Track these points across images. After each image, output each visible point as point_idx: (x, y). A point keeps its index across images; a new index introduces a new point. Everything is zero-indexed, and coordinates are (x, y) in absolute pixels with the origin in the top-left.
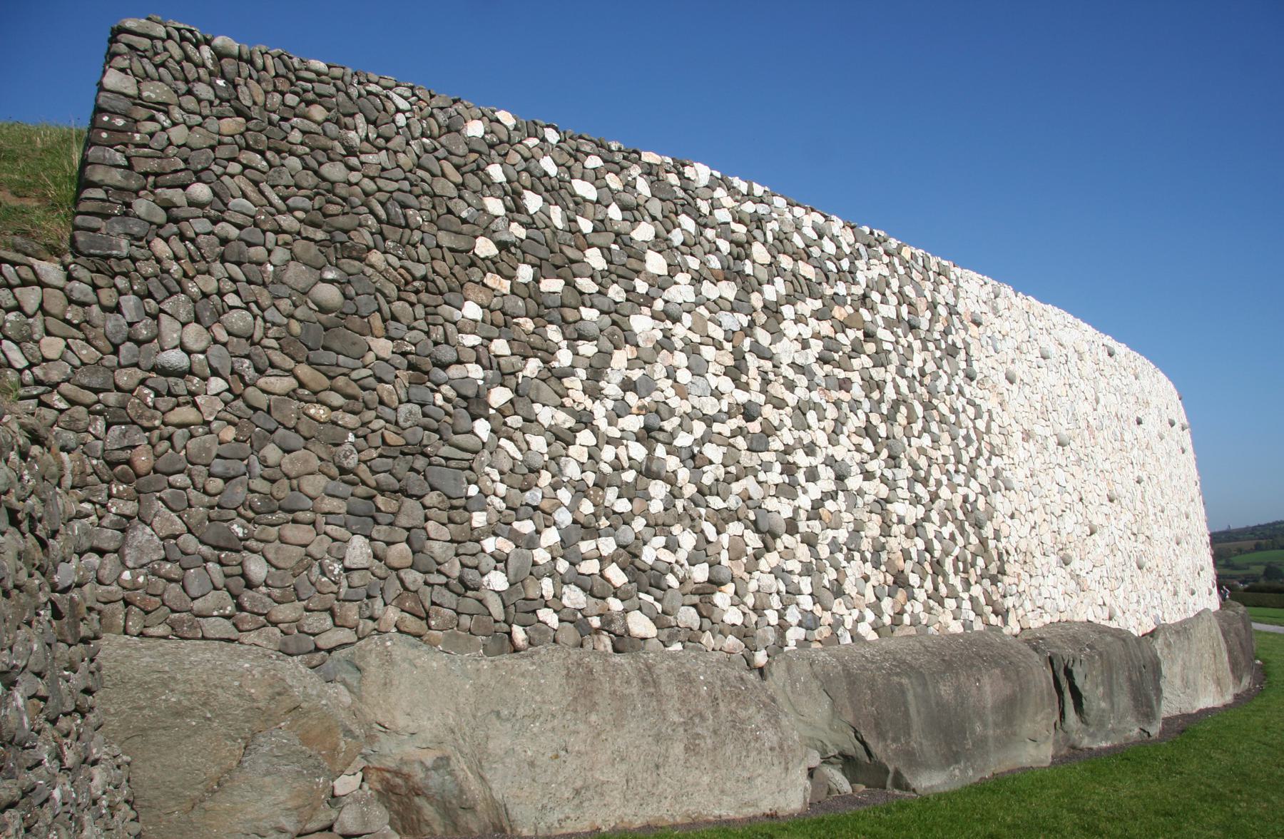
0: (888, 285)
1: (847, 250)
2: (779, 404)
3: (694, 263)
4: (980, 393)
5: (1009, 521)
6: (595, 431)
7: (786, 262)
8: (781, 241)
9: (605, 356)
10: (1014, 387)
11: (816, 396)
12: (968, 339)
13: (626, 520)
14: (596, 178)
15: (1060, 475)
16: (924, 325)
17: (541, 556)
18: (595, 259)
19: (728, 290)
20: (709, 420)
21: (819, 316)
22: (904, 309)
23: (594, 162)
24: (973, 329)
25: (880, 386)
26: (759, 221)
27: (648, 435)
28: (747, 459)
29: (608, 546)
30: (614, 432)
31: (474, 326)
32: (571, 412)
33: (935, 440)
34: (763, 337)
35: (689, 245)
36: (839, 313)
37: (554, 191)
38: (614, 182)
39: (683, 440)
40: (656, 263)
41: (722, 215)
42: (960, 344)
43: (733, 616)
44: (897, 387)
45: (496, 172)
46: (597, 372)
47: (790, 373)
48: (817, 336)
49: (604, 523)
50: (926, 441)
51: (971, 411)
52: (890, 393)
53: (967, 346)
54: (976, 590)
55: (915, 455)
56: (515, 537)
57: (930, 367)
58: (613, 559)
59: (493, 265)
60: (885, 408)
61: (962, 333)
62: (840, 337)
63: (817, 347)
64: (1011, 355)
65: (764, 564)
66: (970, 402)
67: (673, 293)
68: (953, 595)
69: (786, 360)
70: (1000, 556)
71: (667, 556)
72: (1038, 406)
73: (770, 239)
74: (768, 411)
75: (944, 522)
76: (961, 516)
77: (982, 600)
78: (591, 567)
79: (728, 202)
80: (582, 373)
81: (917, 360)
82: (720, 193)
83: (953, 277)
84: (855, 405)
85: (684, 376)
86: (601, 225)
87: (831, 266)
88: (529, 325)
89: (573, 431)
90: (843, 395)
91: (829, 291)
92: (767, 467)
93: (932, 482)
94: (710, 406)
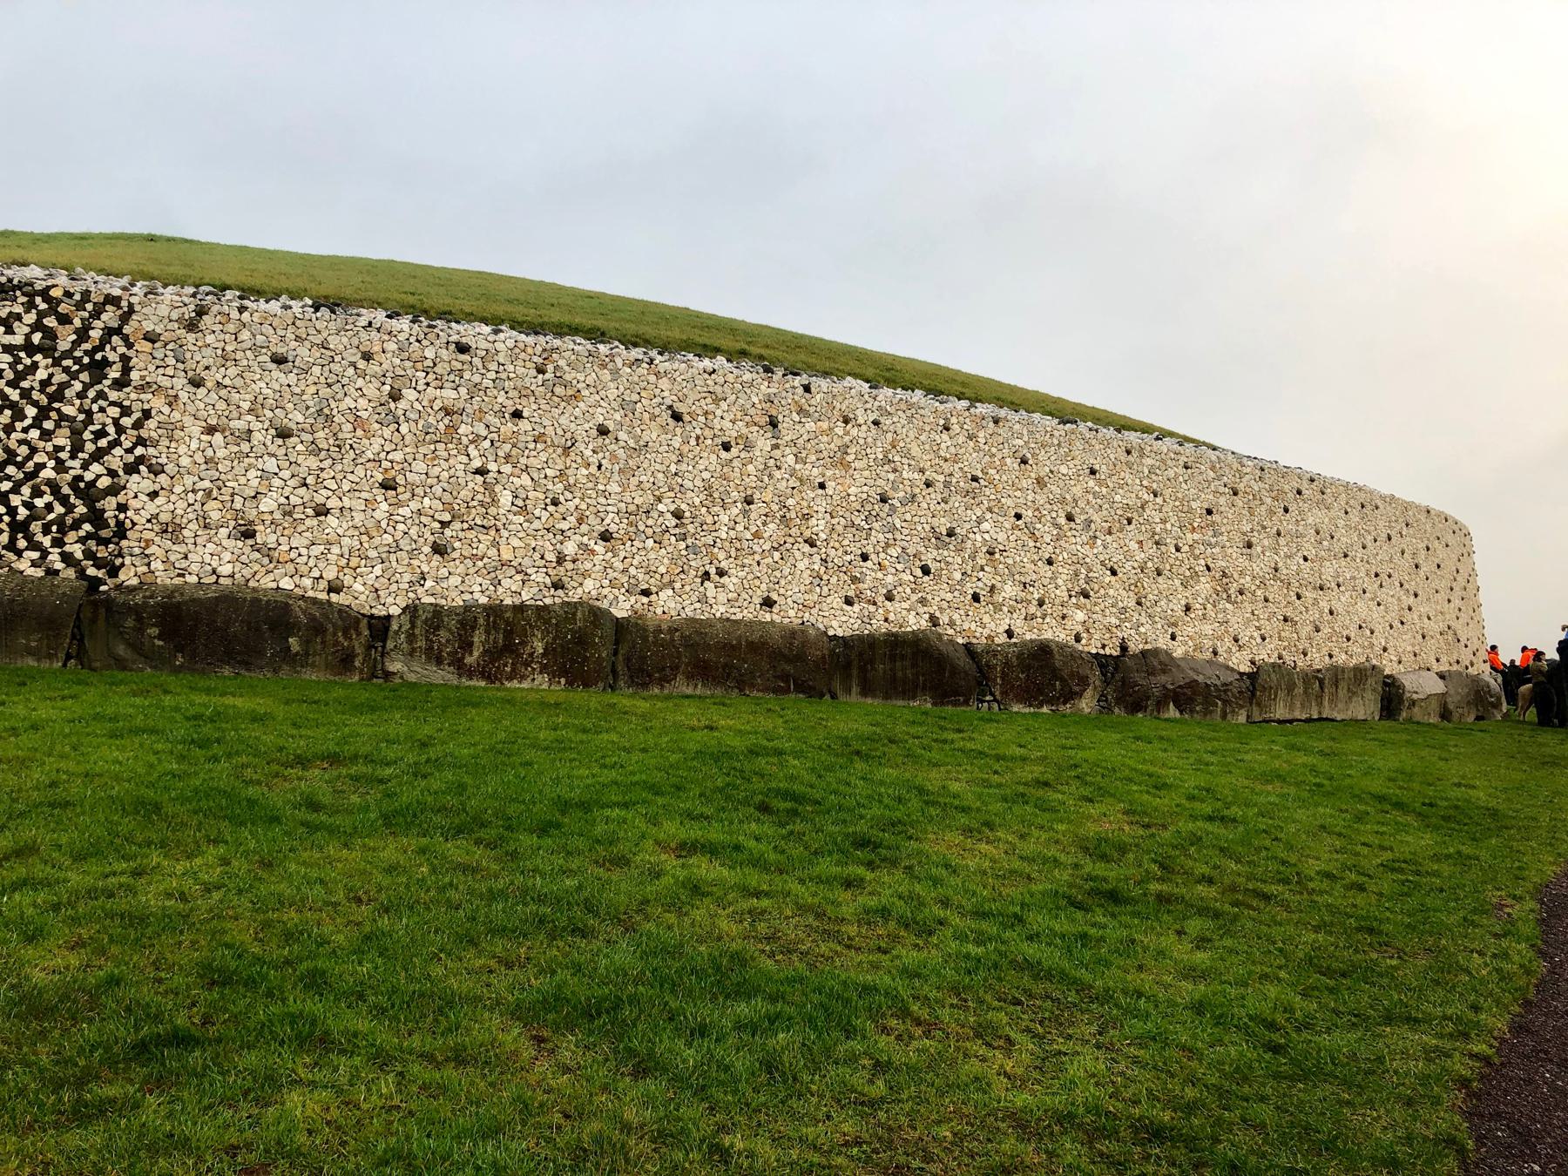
4: (133, 396)
5: (146, 499)
10: (202, 391)
12: (131, 353)
15: (271, 465)
16: (63, 345)
22: (37, 338)
24: (147, 346)
33: (46, 435)
42: (112, 357)
50: (34, 434)
51: (114, 412)
53: (125, 359)
54: (77, 551)
55: (13, 444)
57: (60, 377)
64: (205, 362)
66: (113, 404)
68: (34, 545)
70: (120, 524)
75: (37, 493)
76: (66, 490)
77: (79, 555)
81: (42, 374)
83: (124, 304)
93: (31, 464)
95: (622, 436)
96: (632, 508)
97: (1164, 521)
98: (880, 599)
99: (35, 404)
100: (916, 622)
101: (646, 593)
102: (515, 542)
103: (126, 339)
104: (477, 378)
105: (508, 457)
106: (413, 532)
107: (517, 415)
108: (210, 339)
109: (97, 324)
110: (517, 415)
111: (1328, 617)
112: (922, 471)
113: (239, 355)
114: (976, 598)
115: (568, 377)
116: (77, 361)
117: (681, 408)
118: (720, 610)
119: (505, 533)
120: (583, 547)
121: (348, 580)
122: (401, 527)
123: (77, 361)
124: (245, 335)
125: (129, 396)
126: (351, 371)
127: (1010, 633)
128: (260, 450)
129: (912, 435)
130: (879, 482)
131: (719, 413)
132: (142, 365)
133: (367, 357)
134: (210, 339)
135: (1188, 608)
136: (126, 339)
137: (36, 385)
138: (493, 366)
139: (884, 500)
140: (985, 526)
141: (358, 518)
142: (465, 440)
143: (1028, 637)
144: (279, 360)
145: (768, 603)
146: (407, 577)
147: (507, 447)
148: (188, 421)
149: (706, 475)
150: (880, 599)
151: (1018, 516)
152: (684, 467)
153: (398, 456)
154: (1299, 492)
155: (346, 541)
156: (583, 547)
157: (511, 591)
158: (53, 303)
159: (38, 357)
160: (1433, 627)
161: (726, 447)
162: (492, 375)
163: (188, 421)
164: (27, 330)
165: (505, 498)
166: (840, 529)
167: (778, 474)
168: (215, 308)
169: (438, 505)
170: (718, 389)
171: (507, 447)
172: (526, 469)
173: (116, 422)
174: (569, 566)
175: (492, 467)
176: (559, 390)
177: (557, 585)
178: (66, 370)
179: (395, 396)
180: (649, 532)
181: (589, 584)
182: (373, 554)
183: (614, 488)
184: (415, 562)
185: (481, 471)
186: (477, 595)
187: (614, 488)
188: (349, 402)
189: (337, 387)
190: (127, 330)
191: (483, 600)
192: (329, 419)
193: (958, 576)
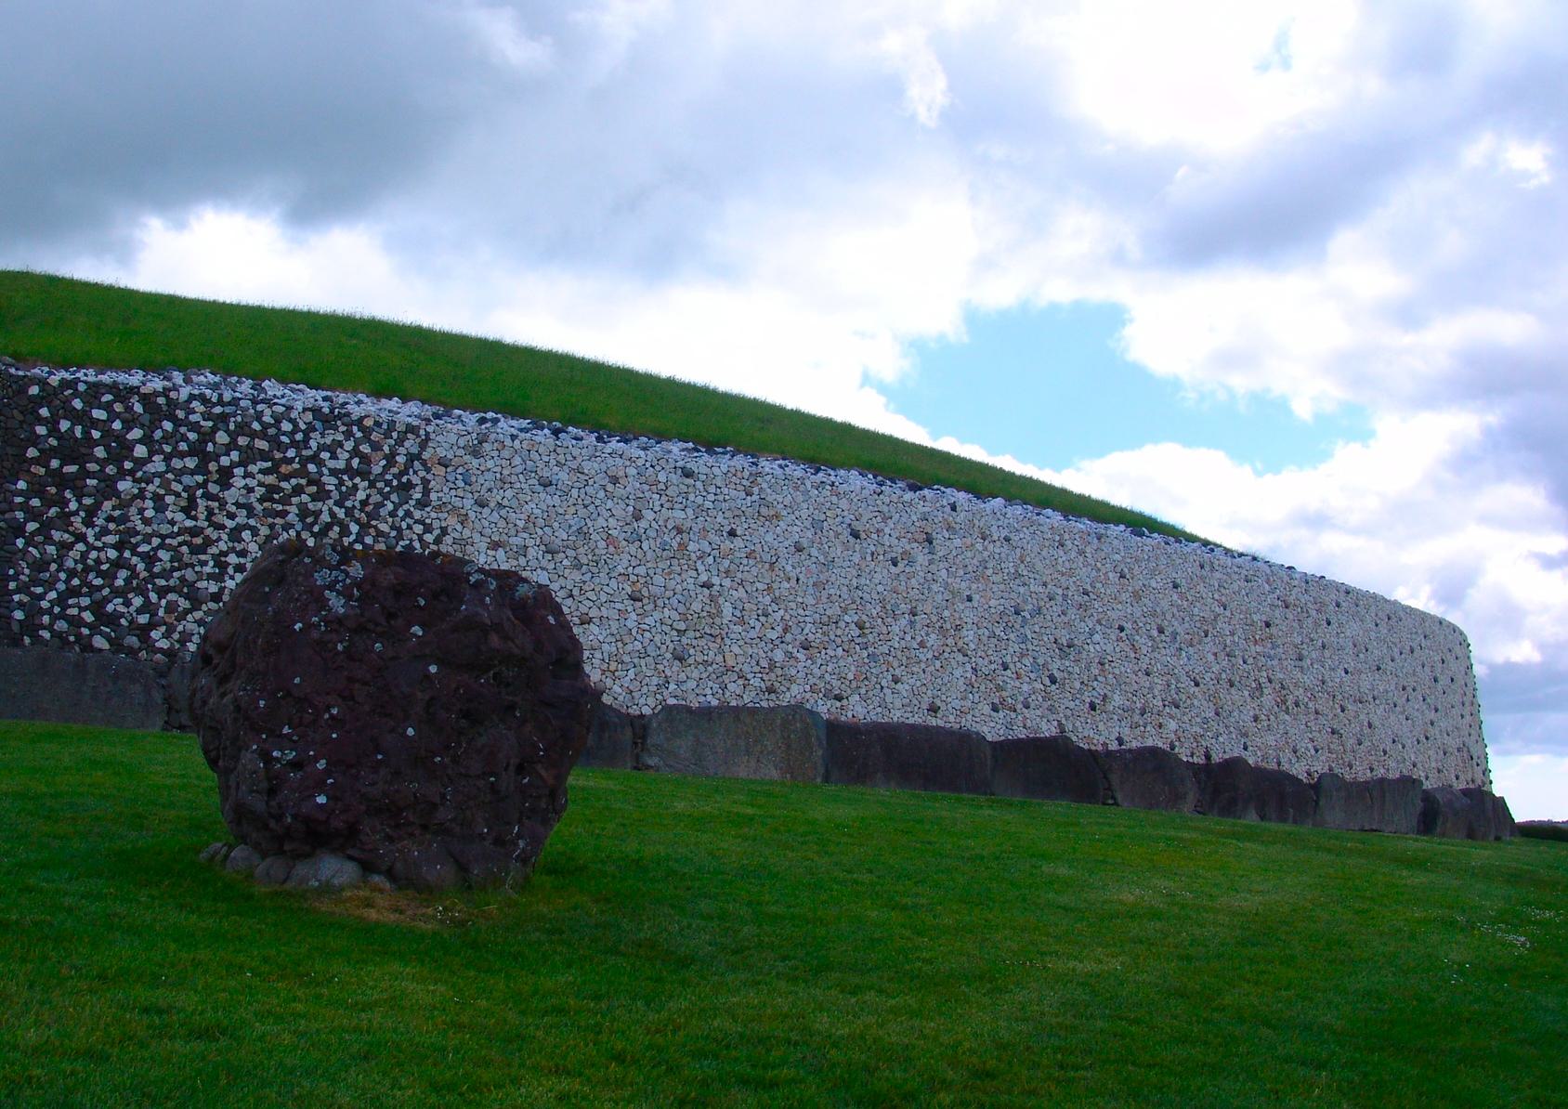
0: (341, 446)
1: (303, 427)
2: (223, 527)
3: (168, 449)
4: (433, 515)
6: (87, 543)
7: (242, 441)
8: (243, 429)
9: (98, 506)
10: (486, 511)
11: (252, 522)
12: (429, 477)
13: (100, 588)
14: (108, 407)
16: (377, 469)
17: (45, 604)
18: (100, 452)
19: (191, 463)
20: (163, 537)
21: (264, 472)
22: (355, 462)
23: (107, 398)
24: (440, 470)
25: (317, 514)
26: (224, 418)
27: (119, 547)
28: (186, 559)
29: (85, 601)
30: (99, 544)
31: (20, 493)
32: (71, 534)
34: (213, 488)
35: (167, 438)
36: (284, 469)
37: (81, 417)
38: (118, 407)
39: (144, 548)
40: (140, 451)
41: (193, 418)
42: (416, 480)
43: (164, 644)
44: (332, 514)
45: (44, 412)
46: (92, 512)
47: (233, 509)
48: (261, 484)
49: (85, 590)
51: (418, 529)
52: (325, 518)
53: (425, 482)
56: (32, 595)
57: (376, 498)
58: (86, 609)
59: (35, 461)
60: (316, 529)
61: (422, 474)
62: (284, 485)
63: (260, 491)
64: (487, 485)
65: (189, 617)
66: (417, 522)
67: (150, 468)
69: (230, 501)
71: (122, 609)
72: (521, 524)
73: (232, 427)
74: (209, 531)
78: (74, 611)
79: (202, 408)
80: (82, 514)
81: (361, 495)
82: (195, 404)
84: (287, 527)
85: (149, 513)
86: (108, 433)
87: (285, 439)
88: (53, 490)
89: (73, 544)
90: (279, 521)
91: (278, 455)
92: (204, 563)
94: (165, 529)
95: (814, 552)
96: (825, 619)
97: (1232, 634)
98: (1019, 706)
99: (358, 522)
100: (1048, 730)
101: (839, 698)
102: (736, 649)
103: (424, 463)
104: (699, 499)
105: (727, 572)
106: (657, 639)
107: (732, 533)
108: (490, 464)
109: (402, 450)
110: (732, 533)
111: (1367, 730)
112: (1045, 584)
113: (514, 478)
114: (1092, 706)
115: (769, 499)
116: (388, 483)
117: (857, 526)
118: (896, 716)
119: (728, 642)
120: (790, 655)
121: (609, 682)
122: (647, 635)
123: (388, 483)
124: (517, 461)
125: (430, 515)
126: (602, 494)
127: (1120, 741)
128: (533, 563)
129: (1036, 549)
130: (1014, 595)
131: (887, 530)
132: (438, 487)
133: (615, 480)
134: (490, 464)
135: (1256, 719)
136: (424, 463)
137: (357, 504)
138: (712, 489)
139: (1017, 613)
140: (1097, 637)
141: (614, 625)
142: (693, 557)
143: (1134, 744)
144: (546, 484)
145: (933, 709)
146: (655, 681)
147: (726, 563)
148: (477, 537)
149: (880, 588)
150: (1019, 706)
151: (1121, 629)
152: (863, 581)
153: (641, 570)
154: (1338, 605)
155: (605, 647)
156: (790, 655)
157: (737, 694)
158: (367, 432)
159: (357, 480)
160: (1452, 743)
161: (895, 564)
162: (711, 497)
163: (477, 537)
164: (347, 455)
165: (727, 610)
166: (984, 639)
167: (935, 587)
168: (493, 436)
169: (675, 616)
170: (885, 509)
171: (726, 563)
172: (741, 584)
173: (421, 539)
174: (779, 672)
175: (716, 580)
176: (764, 511)
177: (771, 690)
178: (380, 492)
179: (638, 517)
180: (838, 641)
181: (795, 689)
182: (627, 659)
183: (810, 600)
184: (661, 667)
185: (707, 585)
186: (709, 698)
187: (810, 600)
188: (601, 522)
189: (591, 508)
190: (425, 455)
191: (715, 703)
192: (587, 536)
193: (1077, 685)
